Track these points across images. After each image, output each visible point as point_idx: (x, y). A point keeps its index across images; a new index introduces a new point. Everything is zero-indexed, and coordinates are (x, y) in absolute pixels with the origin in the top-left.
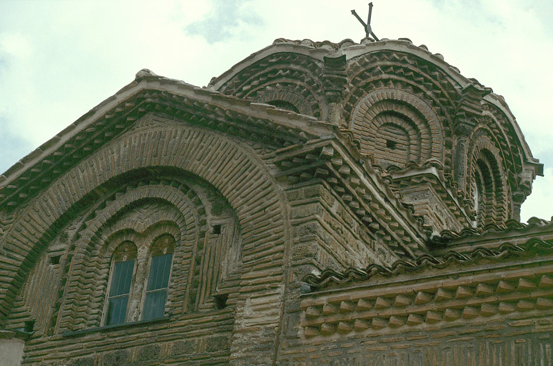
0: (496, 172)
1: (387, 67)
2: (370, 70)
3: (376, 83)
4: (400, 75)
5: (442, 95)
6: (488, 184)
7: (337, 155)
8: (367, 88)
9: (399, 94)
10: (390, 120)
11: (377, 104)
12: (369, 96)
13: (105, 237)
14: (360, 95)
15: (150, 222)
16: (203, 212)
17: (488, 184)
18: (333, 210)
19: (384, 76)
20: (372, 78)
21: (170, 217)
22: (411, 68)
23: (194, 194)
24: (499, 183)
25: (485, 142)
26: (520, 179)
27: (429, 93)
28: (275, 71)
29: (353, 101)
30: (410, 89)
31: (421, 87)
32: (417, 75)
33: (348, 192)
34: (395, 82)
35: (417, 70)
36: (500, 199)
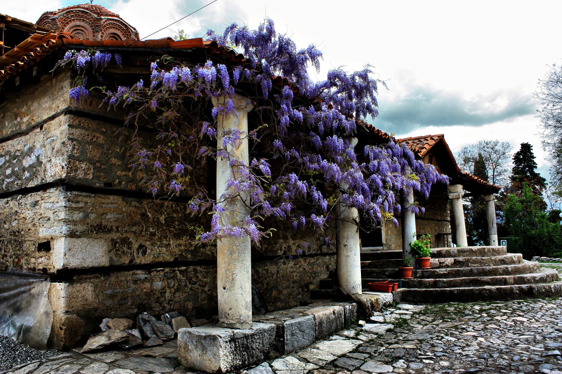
1: (73, 16)
2: (68, 18)
3: (70, 21)
4: (77, 17)
5: (91, 21)
8: (67, 23)
9: (78, 23)
11: (71, 28)
12: (68, 26)
14: (65, 26)
19: (73, 19)
22: (80, 14)
27: (87, 21)
28: (45, 22)
31: (85, 19)
32: (83, 16)
34: (77, 19)
35: (82, 14)
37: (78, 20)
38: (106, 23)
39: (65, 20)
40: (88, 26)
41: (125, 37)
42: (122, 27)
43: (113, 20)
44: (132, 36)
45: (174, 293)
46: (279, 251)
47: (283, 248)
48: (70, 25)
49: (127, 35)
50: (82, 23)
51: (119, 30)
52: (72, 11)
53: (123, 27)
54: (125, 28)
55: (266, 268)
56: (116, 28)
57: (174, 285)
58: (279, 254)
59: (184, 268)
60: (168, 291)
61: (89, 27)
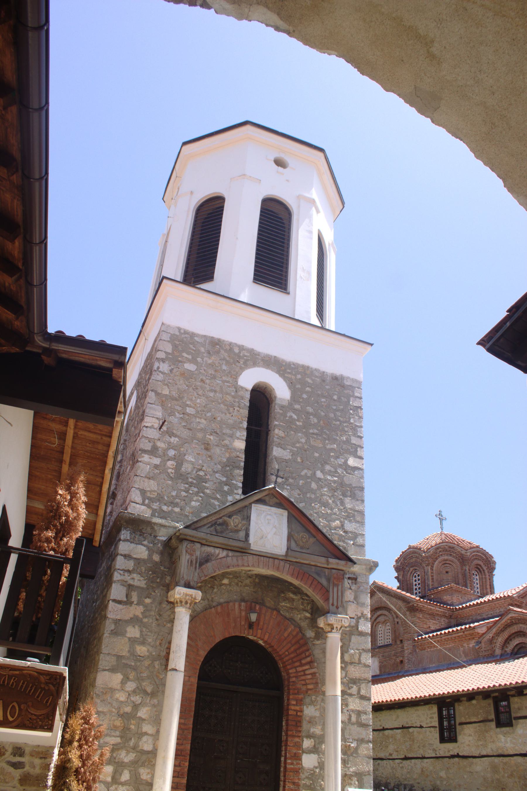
0: (482, 568)
3: (439, 556)
6: (480, 571)
7: (417, 605)
8: (437, 559)
9: (446, 557)
10: (445, 565)
11: (440, 562)
12: (437, 561)
13: (375, 624)
14: (435, 561)
15: (383, 620)
16: (394, 618)
17: (480, 571)
18: (421, 617)
19: (441, 553)
20: (437, 555)
21: (388, 619)
23: (391, 613)
24: (484, 571)
25: (476, 562)
26: (491, 566)
27: (454, 555)
28: (412, 556)
29: (433, 564)
30: (449, 555)
31: (452, 553)
33: (423, 611)
34: (444, 554)
35: (449, 549)
36: (485, 575)
39: (434, 556)
40: (455, 560)
41: (486, 566)
42: (482, 557)
44: (492, 564)
48: (439, 560)
49: (488, 564)
50: (450, 558)
51: (480, 560)
53: (483, 556)
56: (478, 559)
61: (456, 561)
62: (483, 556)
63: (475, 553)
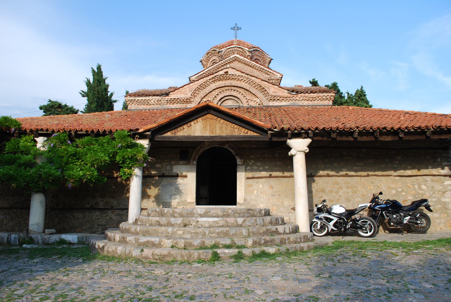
2: (208, 57)
14: (208, 63)
19: (211, 56)
22: (213, 52)
37: (214, 56)
38: (226, 52)
43: (231, 48)
45: (8, 222)
46: (87, 205)
47: (91, 203)
52: (209, 52)
53: (240, 49)
54: (241, 50)
55: (73, 214)
57: (9, 218)
58: (86, 207)
59: (15, 211)
60: (5, 220)
62: (240, 49)
63: (231, 49)
